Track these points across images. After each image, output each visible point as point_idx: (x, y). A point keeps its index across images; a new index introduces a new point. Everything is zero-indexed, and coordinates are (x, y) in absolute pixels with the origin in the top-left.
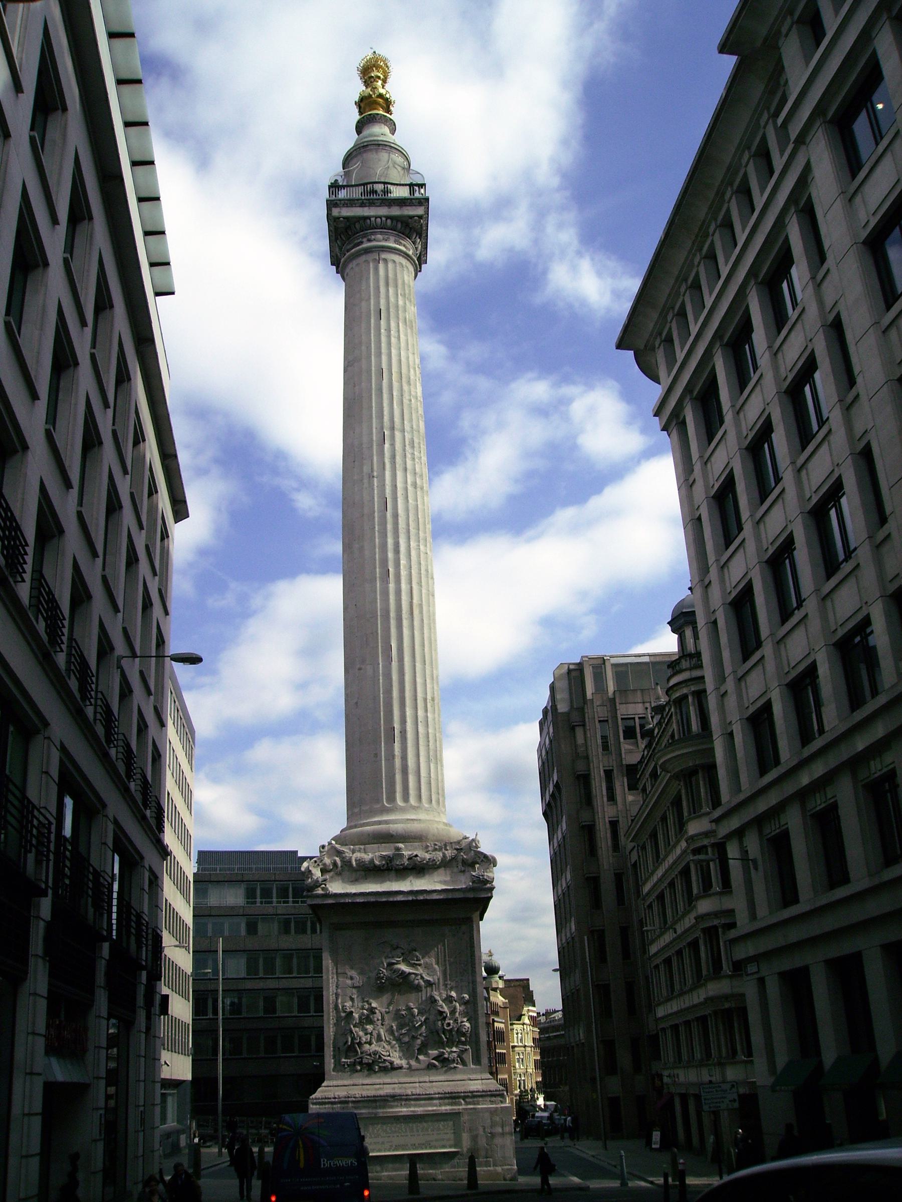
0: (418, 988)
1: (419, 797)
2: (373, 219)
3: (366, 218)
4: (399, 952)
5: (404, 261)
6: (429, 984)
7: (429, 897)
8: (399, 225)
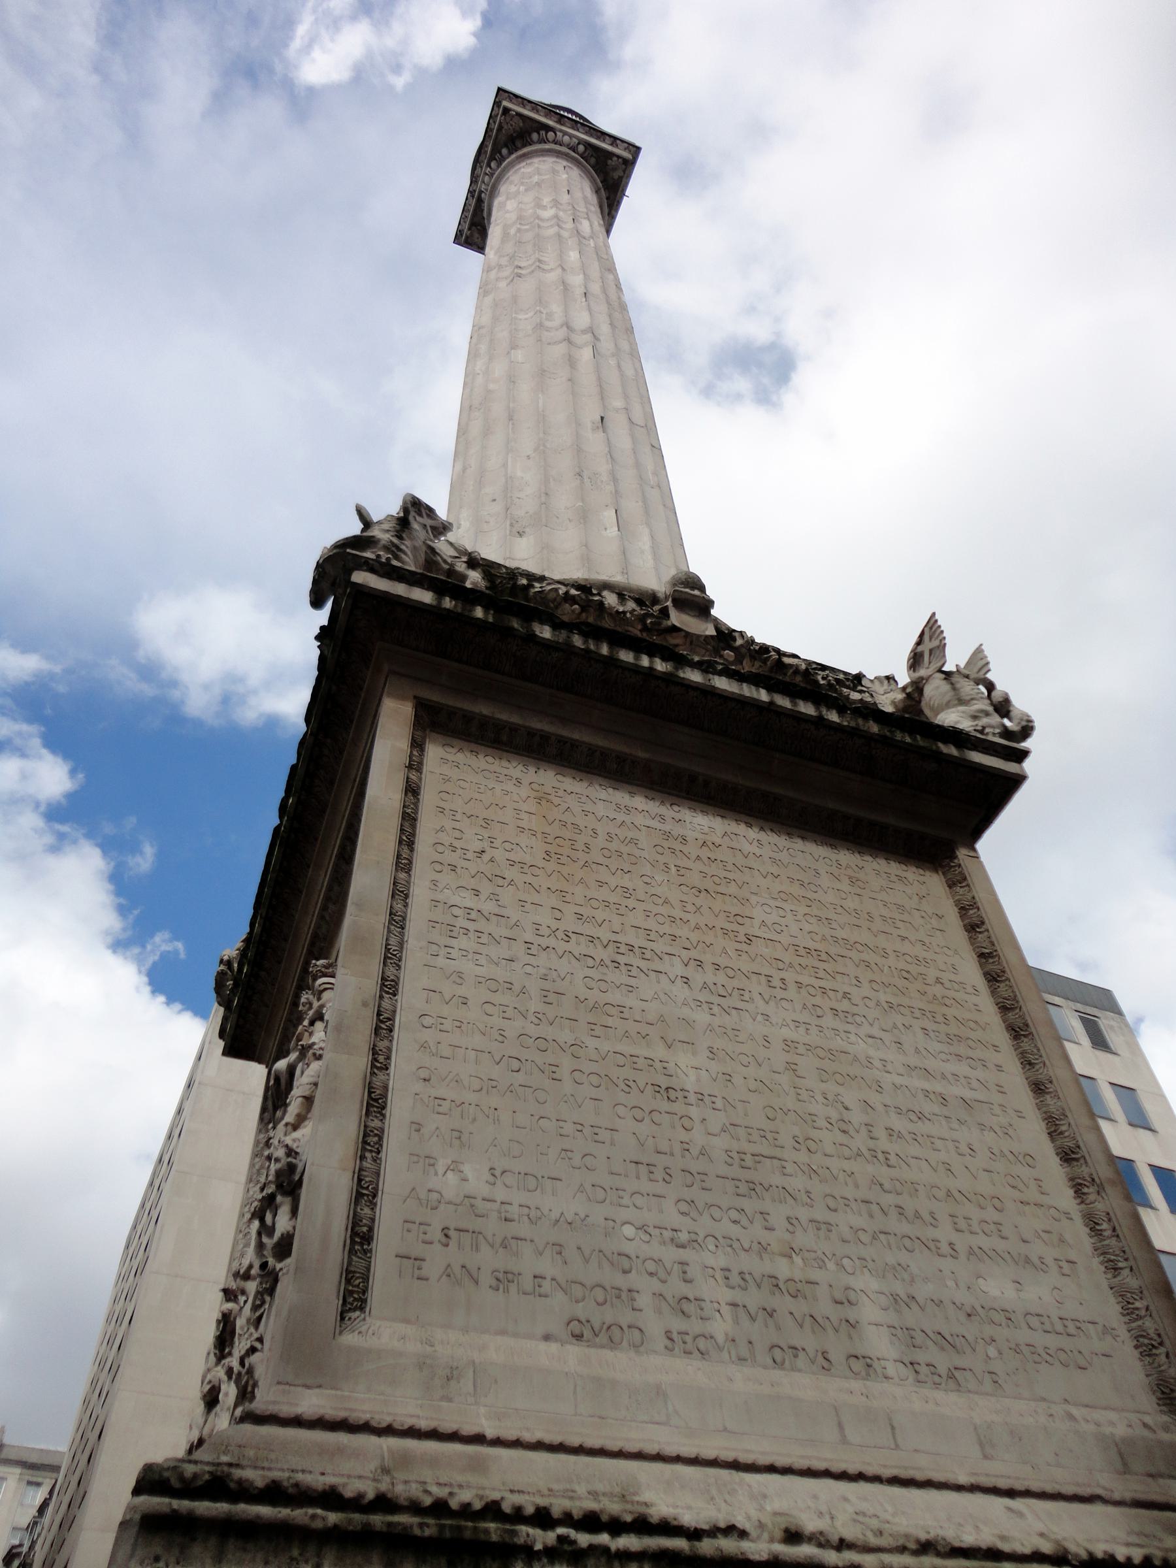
8: (504, 151)
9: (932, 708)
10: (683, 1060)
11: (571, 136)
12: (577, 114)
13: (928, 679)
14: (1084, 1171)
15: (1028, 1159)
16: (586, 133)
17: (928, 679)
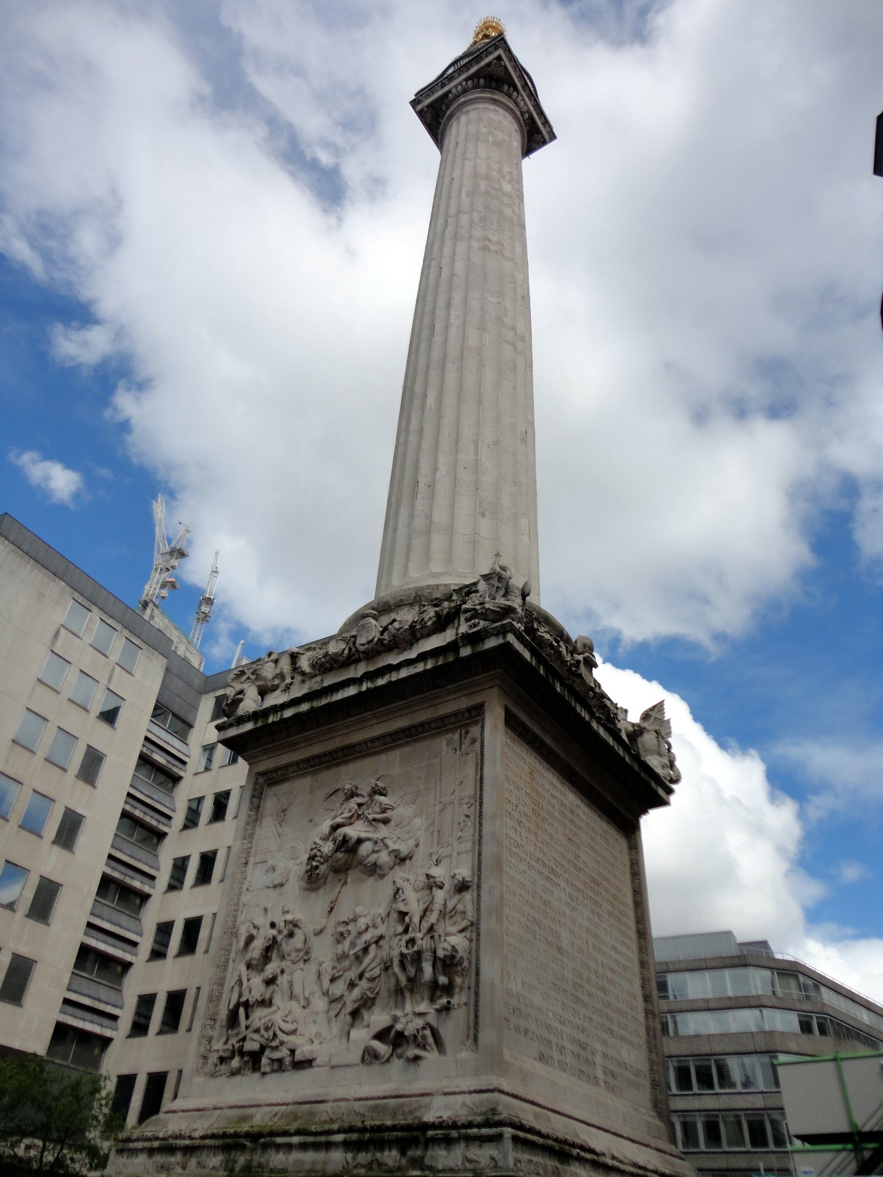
0: (374, 870)
1: (449, 560)
2: (454, 91)
3: (446, 95)
4: (353, 803)
5: (492, 107)
6: (401, 860)
7: (394, 677)
8: (482, 81)
9: (647, 751)
10: (564, 934)
11: (525, 104)
12: (536, 93)
13: (648, 731)
14: (650, 1007)
15: (634, 997)
16: (534, 106)
17: (648, 731)
